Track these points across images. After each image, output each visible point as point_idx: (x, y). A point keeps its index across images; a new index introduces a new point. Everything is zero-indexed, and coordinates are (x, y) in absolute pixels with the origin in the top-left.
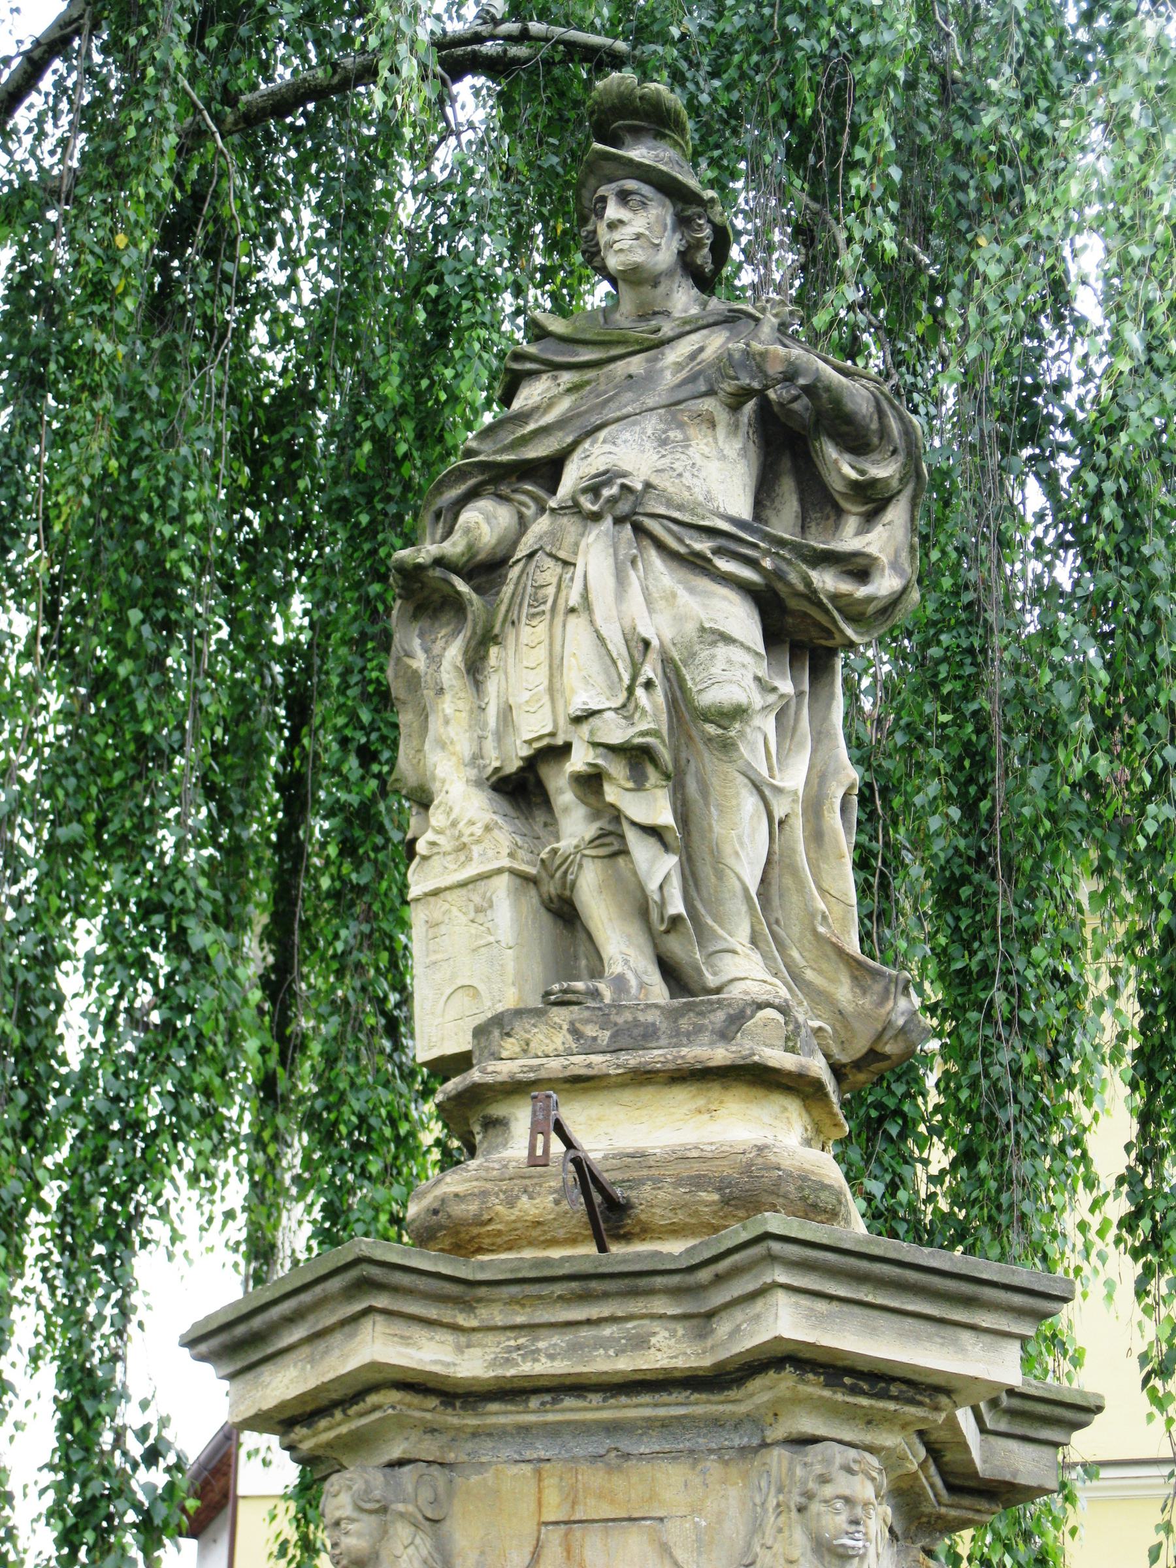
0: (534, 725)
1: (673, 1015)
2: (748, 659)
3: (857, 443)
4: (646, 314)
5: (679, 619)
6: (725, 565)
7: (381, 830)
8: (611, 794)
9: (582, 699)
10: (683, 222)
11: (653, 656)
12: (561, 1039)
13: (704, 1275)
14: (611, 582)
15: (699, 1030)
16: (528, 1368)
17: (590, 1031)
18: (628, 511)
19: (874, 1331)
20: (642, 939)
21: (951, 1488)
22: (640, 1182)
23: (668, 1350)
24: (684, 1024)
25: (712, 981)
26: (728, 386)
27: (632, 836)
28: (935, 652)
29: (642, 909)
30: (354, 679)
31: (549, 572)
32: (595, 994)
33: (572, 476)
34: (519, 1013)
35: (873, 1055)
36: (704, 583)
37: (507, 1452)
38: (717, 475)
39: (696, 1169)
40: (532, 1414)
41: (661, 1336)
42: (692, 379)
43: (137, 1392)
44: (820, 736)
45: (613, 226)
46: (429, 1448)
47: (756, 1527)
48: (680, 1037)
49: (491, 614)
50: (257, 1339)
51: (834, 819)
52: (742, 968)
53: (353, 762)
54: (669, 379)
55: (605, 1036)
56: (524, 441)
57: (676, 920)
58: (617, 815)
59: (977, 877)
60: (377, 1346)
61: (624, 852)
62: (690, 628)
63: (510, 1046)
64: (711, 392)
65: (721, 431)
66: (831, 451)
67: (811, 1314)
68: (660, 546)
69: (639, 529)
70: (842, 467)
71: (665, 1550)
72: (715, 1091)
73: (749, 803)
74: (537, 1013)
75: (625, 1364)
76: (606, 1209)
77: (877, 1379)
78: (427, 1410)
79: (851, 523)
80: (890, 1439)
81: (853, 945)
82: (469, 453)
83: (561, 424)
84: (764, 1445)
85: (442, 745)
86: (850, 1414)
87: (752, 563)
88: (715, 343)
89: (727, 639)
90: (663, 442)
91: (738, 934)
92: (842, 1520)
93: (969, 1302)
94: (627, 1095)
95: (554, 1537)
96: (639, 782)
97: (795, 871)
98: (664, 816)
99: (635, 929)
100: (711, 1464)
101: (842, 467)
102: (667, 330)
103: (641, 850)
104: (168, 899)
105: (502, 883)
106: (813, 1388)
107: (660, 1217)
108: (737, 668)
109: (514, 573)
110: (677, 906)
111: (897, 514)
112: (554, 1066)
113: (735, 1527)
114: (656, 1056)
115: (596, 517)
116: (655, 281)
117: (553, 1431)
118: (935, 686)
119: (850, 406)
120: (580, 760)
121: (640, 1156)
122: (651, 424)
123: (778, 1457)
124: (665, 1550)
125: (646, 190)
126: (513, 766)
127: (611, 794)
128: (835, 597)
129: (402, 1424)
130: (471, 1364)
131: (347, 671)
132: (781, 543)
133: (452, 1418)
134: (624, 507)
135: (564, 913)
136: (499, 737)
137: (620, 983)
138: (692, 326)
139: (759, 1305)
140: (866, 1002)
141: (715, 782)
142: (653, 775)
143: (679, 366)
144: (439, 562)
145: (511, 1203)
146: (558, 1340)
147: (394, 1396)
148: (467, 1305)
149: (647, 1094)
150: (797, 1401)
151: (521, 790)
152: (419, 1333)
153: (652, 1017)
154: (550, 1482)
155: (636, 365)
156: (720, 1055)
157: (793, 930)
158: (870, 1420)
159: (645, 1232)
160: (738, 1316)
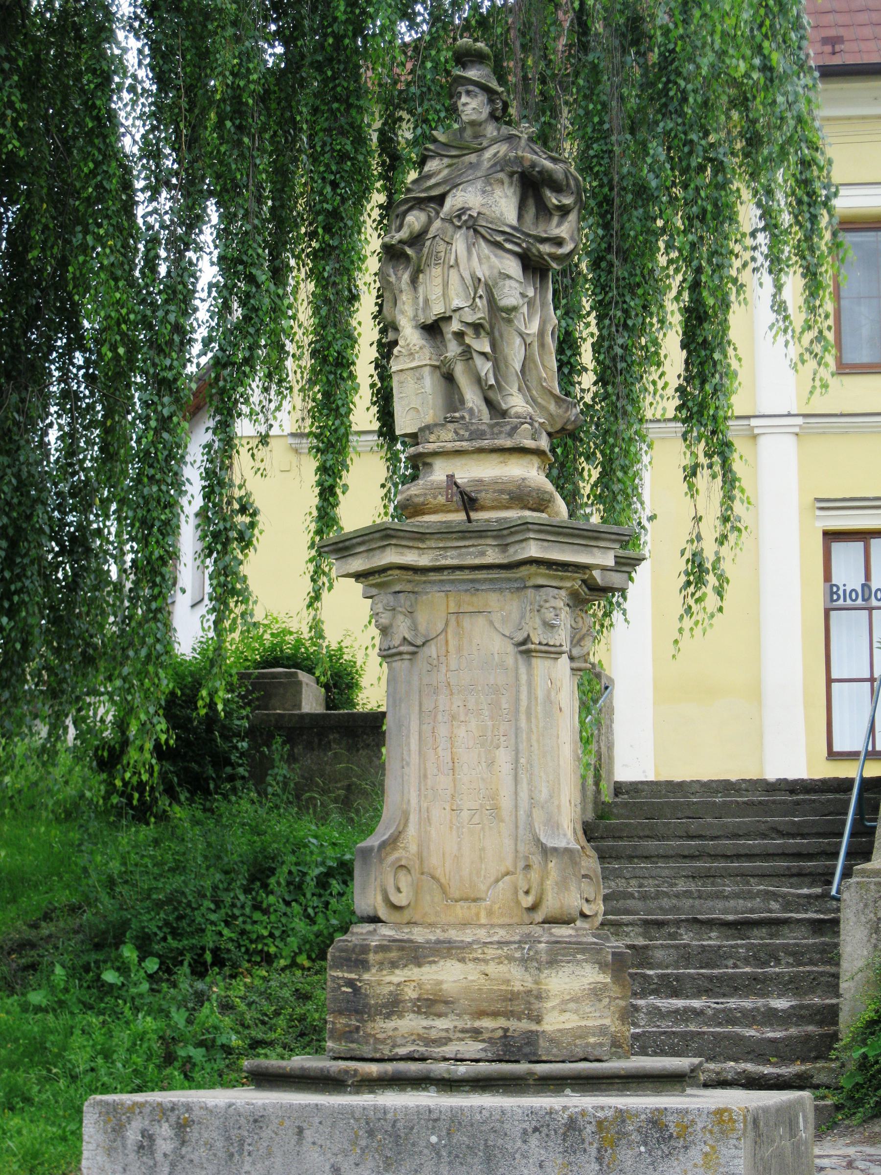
0: (437, 309)
1: (492, 426)
2: (516, 285)
3: (558, 188)
4: (476, 136)
5: (491, 267)
6: (508, 246)
7: (342, 219)
8: (468, 340)
9: (457, 303)
10: (491, 101)
11: (482, 285)
12: (451, 435)
13: (505, 532)
14: (465, 253)
15: (501, 432)
16: (443, 562)
17: (462, 432)
18: (472, 224)
19: (563, 551)
20: (479, 392)
21: (590, 589)
22: (480, 491)
23: (492, 556)
24: (496, 430)
25: (504, 407)
26: (508, 169)
27: (475, 355)
28: (591, 153)
29: (479, 381)
30: (327, 148)
31: (442, 247)
32: (463, 418)
33: (451, 203)
34: (436, 425)
35: (563, 429)
36: (501, 253)
37: (436, 588)
38: (504, 205)
39: (500, 487)
40: (445, 576)
41: (490, 552)
42: (495, 165)
43: (237, 481)
44: (543, 305)
45: (464, 105)
46: (409, 587)
47: (523, 617)
48: (494, 436)
49: (420, 259)
50: (346, 548)
51: (549, 339)
52: (516, 402)
53: (328, 189)
54: (486, 165)
55: (467, 434)
56: (430, 188)
57: (491, 386)
58: (469, 346)
59: (609, 257)
60: (391, 557)
61: (472, 358)
62: (496, 272)
63: (432, 438)
64: (502, 170)
65: (506, 185)
66: (548, 193)
67: (542, 547)
68: (484, 237)
69: (476, 231)
70: (553, 200)
71: (491, 623)
72: (507, 456)
73: (518, 341)
74: (443, 425)
75: (477, 561)
76: (469, 502)
77: (564, 566)
78: (409, 575)
79: (555, 220)
80: (568, 584)
81: (557, 391)
82: (409, 190)
83: (444, 182)
84: (525, 587)
85: (402, 312)
86: (555, 577)
87: (519, 245)
88: (502, 149)
89: (509, 277)
90: (484, 192)
91: (514, 390)
92: (552, 615)
93: (596, 539)
94: (475, 456)
95: (453, 618)
96: (477, 335)
97: (534, 362)
98: (487, 349)
99: (476, 388)
100: (507, 594)
101: (553, 200)
102: (485, 144)
103: (479, 361)
104: (245, 258)
105: (427, 370)
106: (543, 570)
107: (488, 503)
108: (514, 290)
109: (428, 243)
110: (492, 381)
111: (573, 217)
112: (449, 446)
113: (515, 616)
114: (485, 443)
115: (460, 227)
116: (480, 124)
117: (452, 582)
118: (591, 169)
119: (555, 177)
120: (455, 326)
121: (480, 481)
122: (479, 184)
123: (530, 592)
124: (491, 623)
125: (477, 90)
126: (429, 322)
127: (468, 340)
128: (550, 255)
129: (399, 580)
130: (424, 560)
131: (324, 144)
132: (529, 235)
133: (417, 578)
134: (470, 223)
135: (449, 378)
136: (424, 310)
137: (471, 411)
138: (494, 141)
139: (524, 544)
140: (560, 411)
141: (505, 335)
142: (483, 334)
143: (490, 159)
144: (400, 242)
145: (435, 498)
146: (454, 553)
147: (397, 572)
148: (422, 540)
149: (482, 456)
150: (537, 574)
151: (433, 330)
152: (406, 551)
153: (484, 427)
154: (451, 599)
155: (473, 158)
156: (508, 443)
157: (533, 384)
158: (562, 579)
159: (483, 508)
160: (517, 547)
